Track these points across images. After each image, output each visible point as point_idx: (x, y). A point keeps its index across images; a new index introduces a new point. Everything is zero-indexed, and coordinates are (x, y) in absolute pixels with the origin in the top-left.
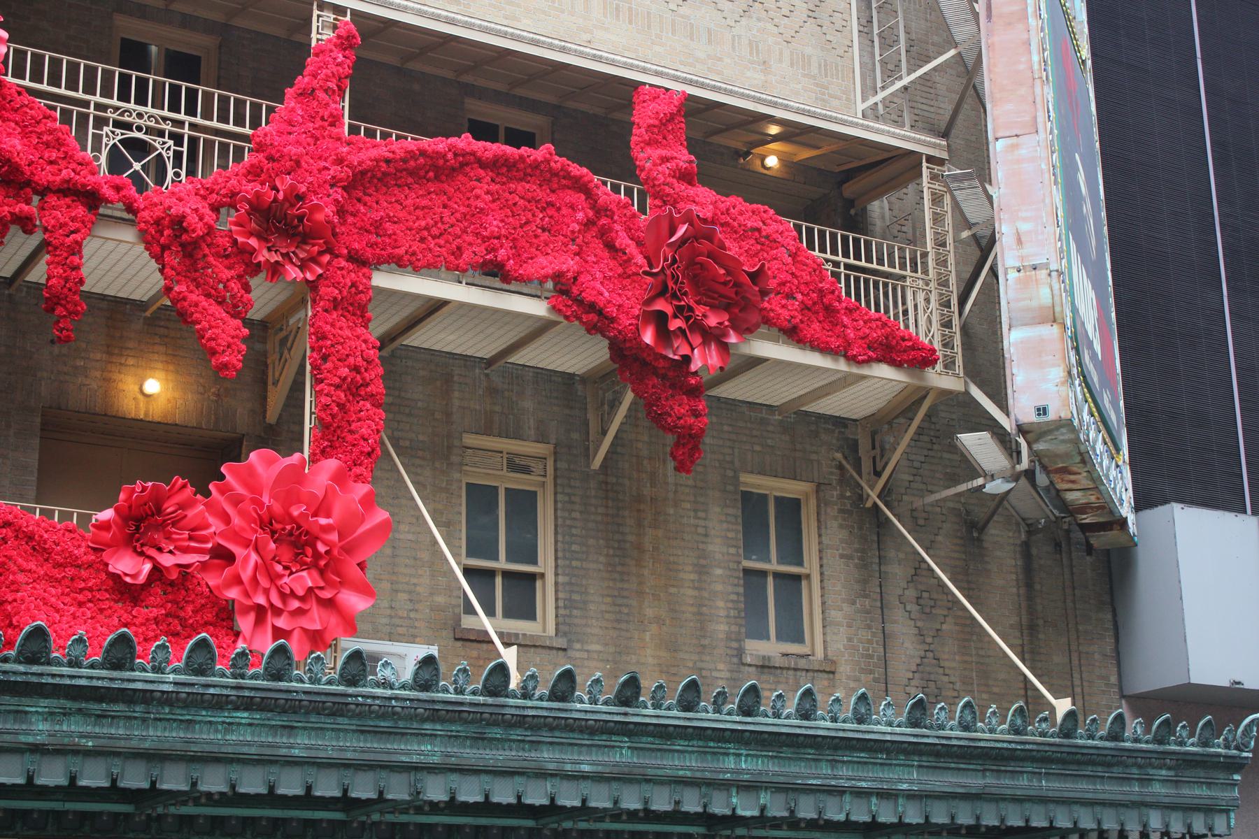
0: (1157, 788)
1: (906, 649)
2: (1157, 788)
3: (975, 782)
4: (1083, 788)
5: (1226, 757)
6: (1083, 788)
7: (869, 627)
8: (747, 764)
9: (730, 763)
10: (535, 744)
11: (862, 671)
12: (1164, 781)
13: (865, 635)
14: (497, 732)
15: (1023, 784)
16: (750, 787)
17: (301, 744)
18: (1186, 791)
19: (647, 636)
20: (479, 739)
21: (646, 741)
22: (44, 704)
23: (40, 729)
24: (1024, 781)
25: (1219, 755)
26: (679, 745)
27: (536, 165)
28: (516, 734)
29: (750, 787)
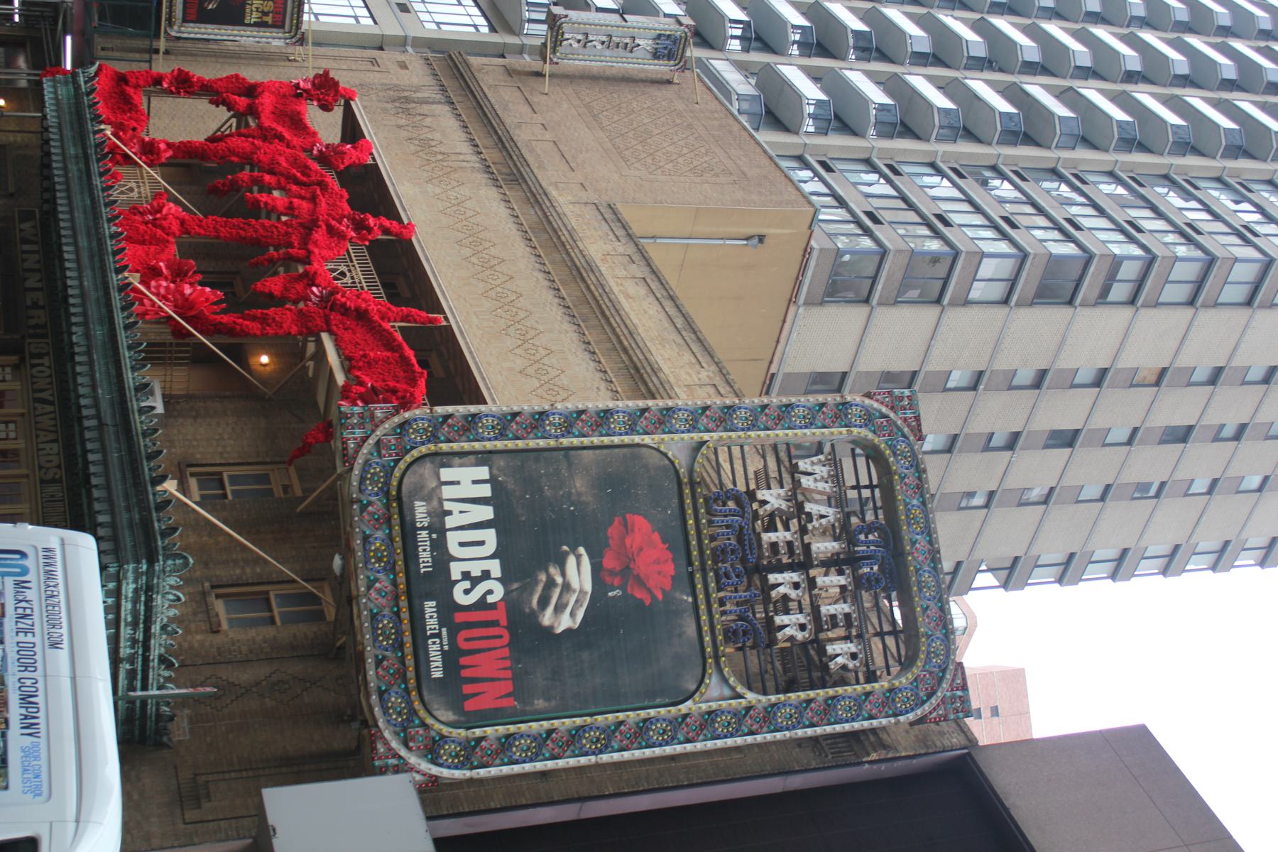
0: (125, 516)
1: (245, 676)
2: (125, 516)
3: (108, 419)
4: (116, 474)
5: (156, 546)
6: (116, 474)
7: (251, 651)
8: (99, 332)
9: (98, 328)
10: (93, 270)
11: (219, 649)
12: (131, 520)
13: (245, 649)
14: (96, 259)
15: (112, 444)
16: (87, 335)
17: (79, 215)
18: (127, 533)
19: (205, 538)
20: (91, 257)
21: (103, 300)
22: (82, 166)
23: (73, 168)
24: (114, 445)
25: (156, 541)
26: (103, 310)
27: (414, 372)
28: (97, 265)
29: (87, 335)
